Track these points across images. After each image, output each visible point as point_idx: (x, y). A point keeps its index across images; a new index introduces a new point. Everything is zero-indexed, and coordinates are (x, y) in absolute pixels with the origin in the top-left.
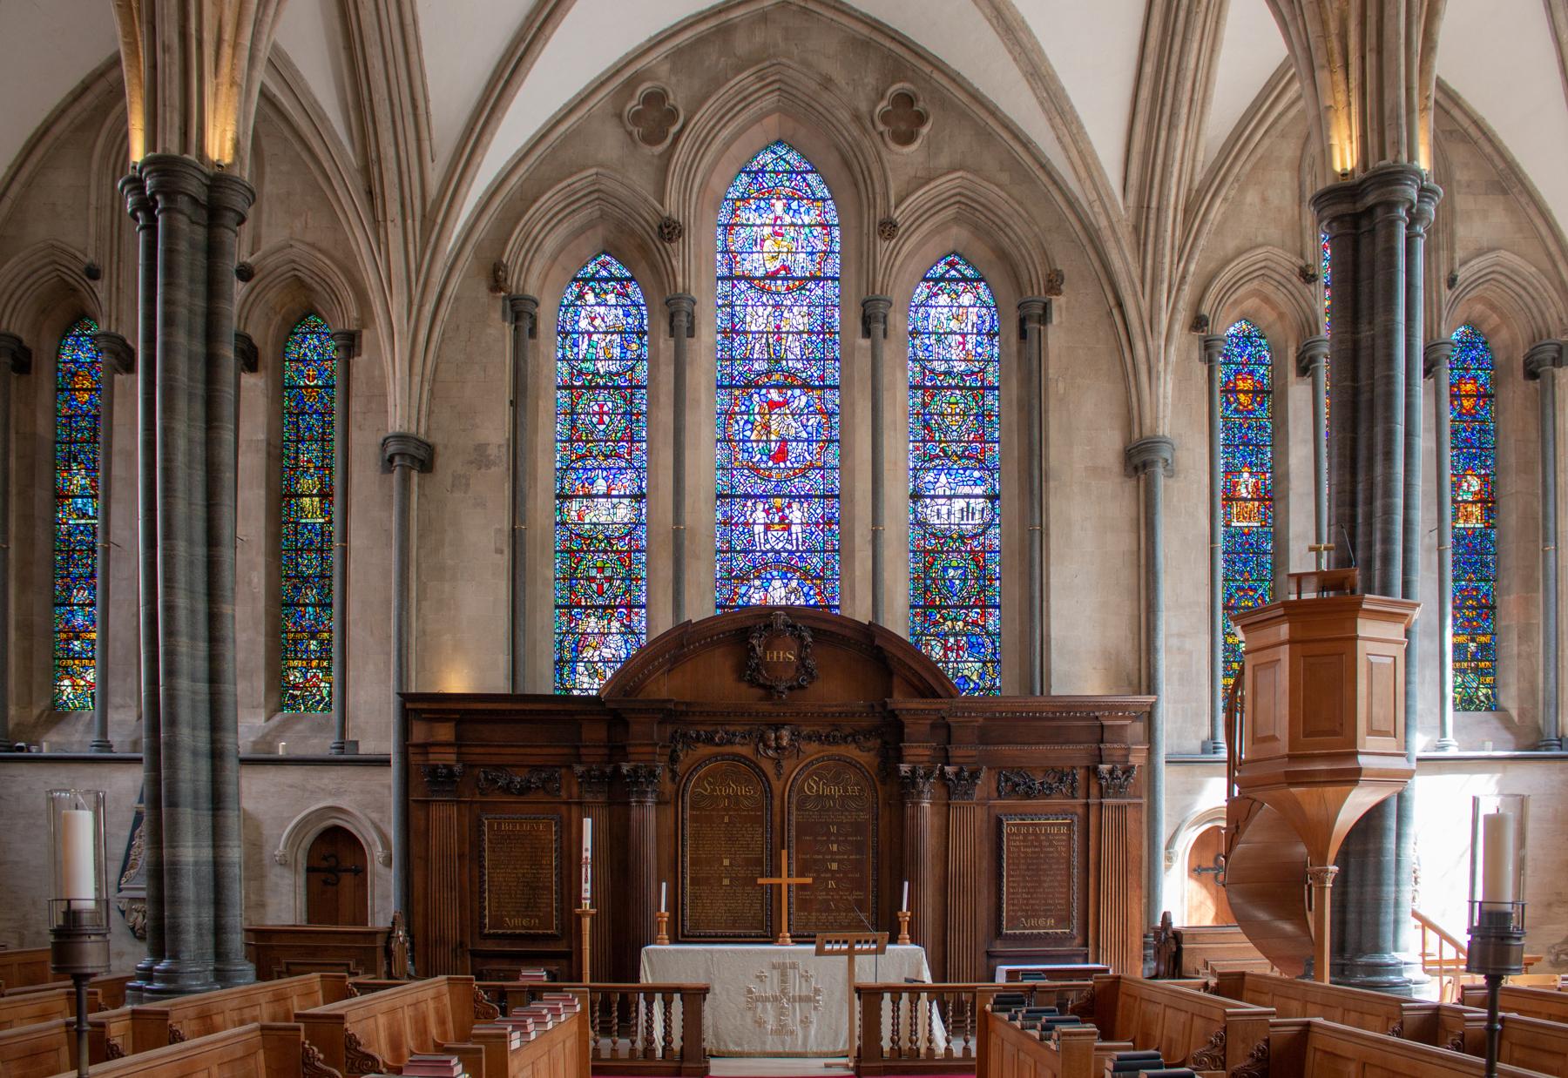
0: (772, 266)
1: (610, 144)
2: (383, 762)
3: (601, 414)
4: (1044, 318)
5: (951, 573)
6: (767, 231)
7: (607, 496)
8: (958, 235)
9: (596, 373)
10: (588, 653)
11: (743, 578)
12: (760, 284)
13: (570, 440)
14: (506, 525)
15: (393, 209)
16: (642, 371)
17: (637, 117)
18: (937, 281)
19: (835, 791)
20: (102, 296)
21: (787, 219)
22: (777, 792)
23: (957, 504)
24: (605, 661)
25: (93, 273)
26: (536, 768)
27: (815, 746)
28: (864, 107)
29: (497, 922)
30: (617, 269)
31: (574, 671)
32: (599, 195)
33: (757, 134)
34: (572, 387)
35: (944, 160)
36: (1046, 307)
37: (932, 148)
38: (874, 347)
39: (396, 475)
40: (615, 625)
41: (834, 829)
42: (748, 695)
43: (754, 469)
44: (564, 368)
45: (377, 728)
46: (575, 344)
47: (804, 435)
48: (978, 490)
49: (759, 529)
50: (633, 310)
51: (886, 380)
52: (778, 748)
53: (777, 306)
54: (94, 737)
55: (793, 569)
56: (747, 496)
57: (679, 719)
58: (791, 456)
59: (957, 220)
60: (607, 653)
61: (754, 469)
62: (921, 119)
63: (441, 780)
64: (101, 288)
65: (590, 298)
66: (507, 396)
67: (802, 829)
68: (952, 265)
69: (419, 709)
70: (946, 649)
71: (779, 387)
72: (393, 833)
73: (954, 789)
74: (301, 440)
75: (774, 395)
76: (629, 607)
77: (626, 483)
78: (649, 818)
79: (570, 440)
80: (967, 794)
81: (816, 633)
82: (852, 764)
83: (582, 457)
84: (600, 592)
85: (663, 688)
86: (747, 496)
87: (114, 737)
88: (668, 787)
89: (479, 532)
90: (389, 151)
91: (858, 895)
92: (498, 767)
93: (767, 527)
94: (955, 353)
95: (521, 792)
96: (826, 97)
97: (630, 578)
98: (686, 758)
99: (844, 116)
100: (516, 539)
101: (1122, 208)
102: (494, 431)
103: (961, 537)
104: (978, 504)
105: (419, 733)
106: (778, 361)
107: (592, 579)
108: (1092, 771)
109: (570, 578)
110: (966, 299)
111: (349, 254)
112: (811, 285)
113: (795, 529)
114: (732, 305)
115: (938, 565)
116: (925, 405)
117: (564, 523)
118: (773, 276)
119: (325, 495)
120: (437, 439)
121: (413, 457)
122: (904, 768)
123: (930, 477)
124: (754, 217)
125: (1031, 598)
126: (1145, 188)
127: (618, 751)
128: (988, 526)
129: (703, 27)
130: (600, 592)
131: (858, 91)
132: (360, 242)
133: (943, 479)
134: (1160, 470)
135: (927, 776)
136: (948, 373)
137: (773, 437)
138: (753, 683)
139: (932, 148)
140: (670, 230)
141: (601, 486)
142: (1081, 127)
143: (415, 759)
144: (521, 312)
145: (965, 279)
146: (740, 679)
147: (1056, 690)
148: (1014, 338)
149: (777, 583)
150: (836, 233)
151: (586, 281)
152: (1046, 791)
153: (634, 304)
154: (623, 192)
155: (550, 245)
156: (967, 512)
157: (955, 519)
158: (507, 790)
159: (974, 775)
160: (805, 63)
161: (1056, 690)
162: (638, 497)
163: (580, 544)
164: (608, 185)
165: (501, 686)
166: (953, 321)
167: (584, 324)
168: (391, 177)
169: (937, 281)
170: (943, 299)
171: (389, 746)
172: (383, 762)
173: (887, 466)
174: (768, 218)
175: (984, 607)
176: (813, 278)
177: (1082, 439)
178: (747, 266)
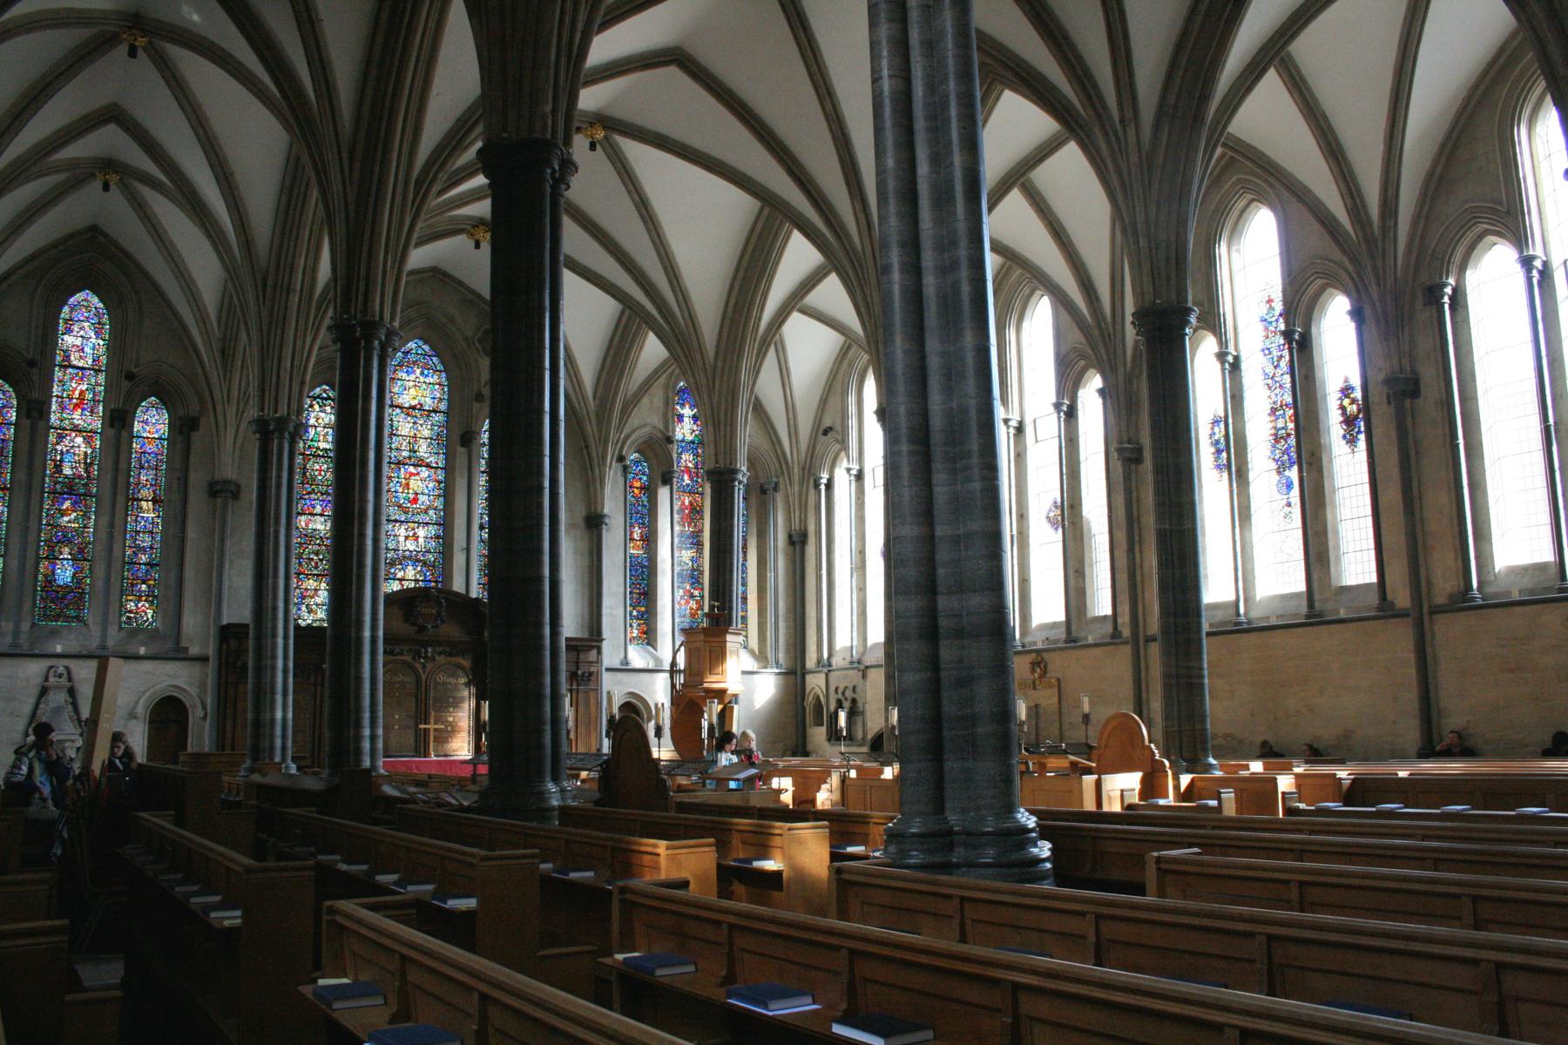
0: (414, 403)
10: (306, 601)
22: (423, 677)
42: (409, 630)
43: (400, 506)
49: (402, 539)
52: (426, 657)
61: (400, 506)
65: (317, 407)
71: (415, 466)
74: (142, 467)
75: (412, 469)
93: (407, 538)
113: (421, 540)
118: (413, 408)
124: (404, 376)
141: (318, 509)
172: (204, 659)
174: (412, 377)
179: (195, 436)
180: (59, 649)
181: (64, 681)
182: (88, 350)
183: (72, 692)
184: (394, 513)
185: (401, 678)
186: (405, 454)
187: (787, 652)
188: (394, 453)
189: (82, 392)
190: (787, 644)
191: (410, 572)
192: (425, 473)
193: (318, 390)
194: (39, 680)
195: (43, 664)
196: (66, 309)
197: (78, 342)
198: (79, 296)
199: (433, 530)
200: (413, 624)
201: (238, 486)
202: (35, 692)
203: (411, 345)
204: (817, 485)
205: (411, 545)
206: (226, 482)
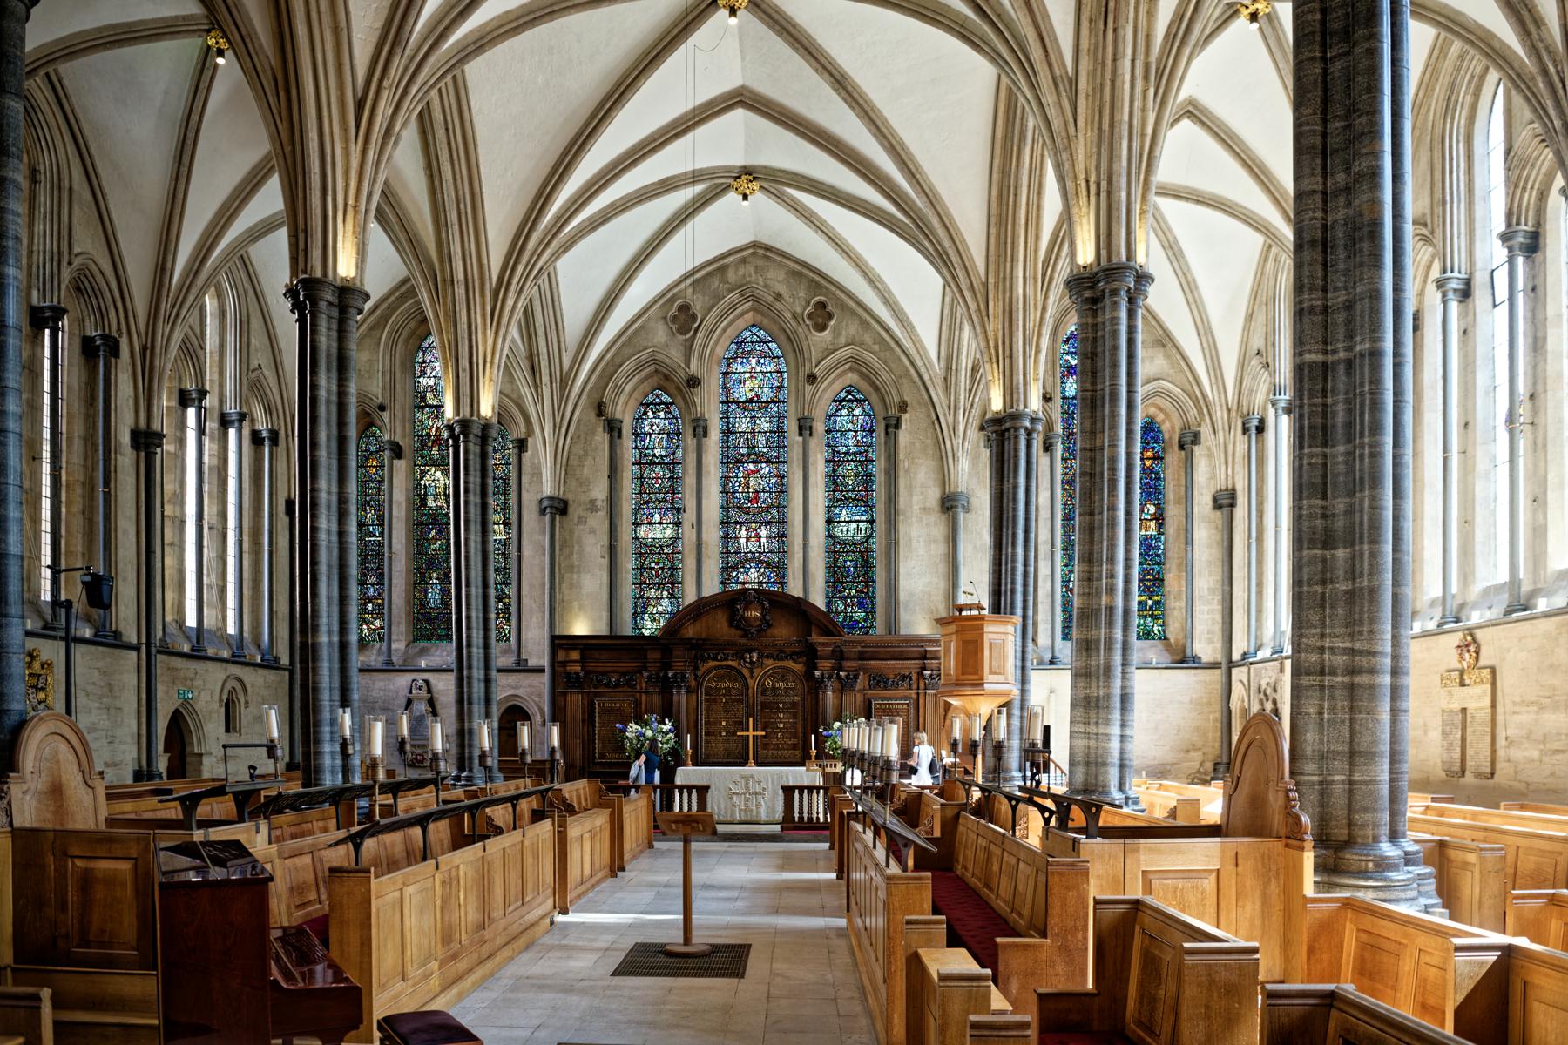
0: (750, 395)
1: (660, 334)
2: (541, 670)
4: (897, 426)
8: (852, 378)
10: (650, 609)
11: (735, 567)
12: (744, 405)
14: (606, 542)
15: (545, 379)
17: (674, 319)
19: (781, 685)
20: (387, 420)
23: (851, 527)
25: (382, 408)
26: (623, 674)
27: (771, 661)
28: (799, 310)
29: (602, 756)
30: (665, 398)
32: (653, 361)
33: (741, 323)
35: (843, 340)
36: (899, 420)
37: (836, 333)
39: (547, 517)
45: (537, 651)
49: (743, 541)
51: (811, 460)
52: (752, 662)
54: (382, 658)
55: (762, 562)
56: (737, 523)
57: (702, 648)
59: (851, 369)
63: (573, 682)
64: (386, 415)
65: (650, 414)
66: (606, 473)
67: (765, 705)
69: (560, 643)
72: (546, 709)
73: (845, 686)
75: (751, 466)
76: (673, 583)
77: (670, 517)
80: (852, 687)
81: (772, 602)
82: (792, 671)
85: (690, 632)
86: (737, 523)
87: (394, 659)
88: (693, 683)
89: (593, 545)
90: (543, 350)
91: (794, 741)
92: (604, 673)
93: (748, 539)
94: (851, 442)
95: (618, 685)
96: (778, 305)
97: (673, 568)
98: (703, 668)
99: (788, 315)
100: (612, 551)
101: (938, 368)
102: (600, 492)
104: (863, 525)
105: (561, 656)
108: (920, 675)
109: (640, 568)
110: (857, 412)
111: (520, 397)
113: (763, 540)
117: (637, 538)
118: (750, 401)
119: (506, 524)
120: (569, 497)
121: (558, 508)
122: (817, 673)
126: (949, 359)
127: (667, 666)
128: (868, 538)
129: (710, 269)
131: (796, 301)
132: (527, 393)
134: (960, 510)
135: (830, 677)
136: (847, 453)
139: (836, 333)
140: (694, 382)
141: (657, 518)
142: (913, 328)
143: (559, 669)
144: (613, 428)
146: (731, 625)
147: (903, 631)
152: (896, 685)
154: (667, 360)
155: (628, 388)
156: (858, 530)
158: (607, 686)
159: (856, 677)
160: (766, 286)
161: (903, 631)
162: (678, 524)
163: (644, 550)
164: (659, 357)
165: (603, 630)
167: (647, 429)
168: (544, 363)
170: (844, 412)
172: (542, 670)
173: (811, 506)
175: (866, 582)
177: (918, 491)
179: (526, 457)
180: (423, 665)
181: (423, 693)
183: (431, 702)
185: (727, 684)
191: (753, 575)
194: (406, 692)
195: (409, 677)
197: (431, 382)
201: (566, 503)
202: (404, 701)
205: (753, 546)
206: (551, 498)
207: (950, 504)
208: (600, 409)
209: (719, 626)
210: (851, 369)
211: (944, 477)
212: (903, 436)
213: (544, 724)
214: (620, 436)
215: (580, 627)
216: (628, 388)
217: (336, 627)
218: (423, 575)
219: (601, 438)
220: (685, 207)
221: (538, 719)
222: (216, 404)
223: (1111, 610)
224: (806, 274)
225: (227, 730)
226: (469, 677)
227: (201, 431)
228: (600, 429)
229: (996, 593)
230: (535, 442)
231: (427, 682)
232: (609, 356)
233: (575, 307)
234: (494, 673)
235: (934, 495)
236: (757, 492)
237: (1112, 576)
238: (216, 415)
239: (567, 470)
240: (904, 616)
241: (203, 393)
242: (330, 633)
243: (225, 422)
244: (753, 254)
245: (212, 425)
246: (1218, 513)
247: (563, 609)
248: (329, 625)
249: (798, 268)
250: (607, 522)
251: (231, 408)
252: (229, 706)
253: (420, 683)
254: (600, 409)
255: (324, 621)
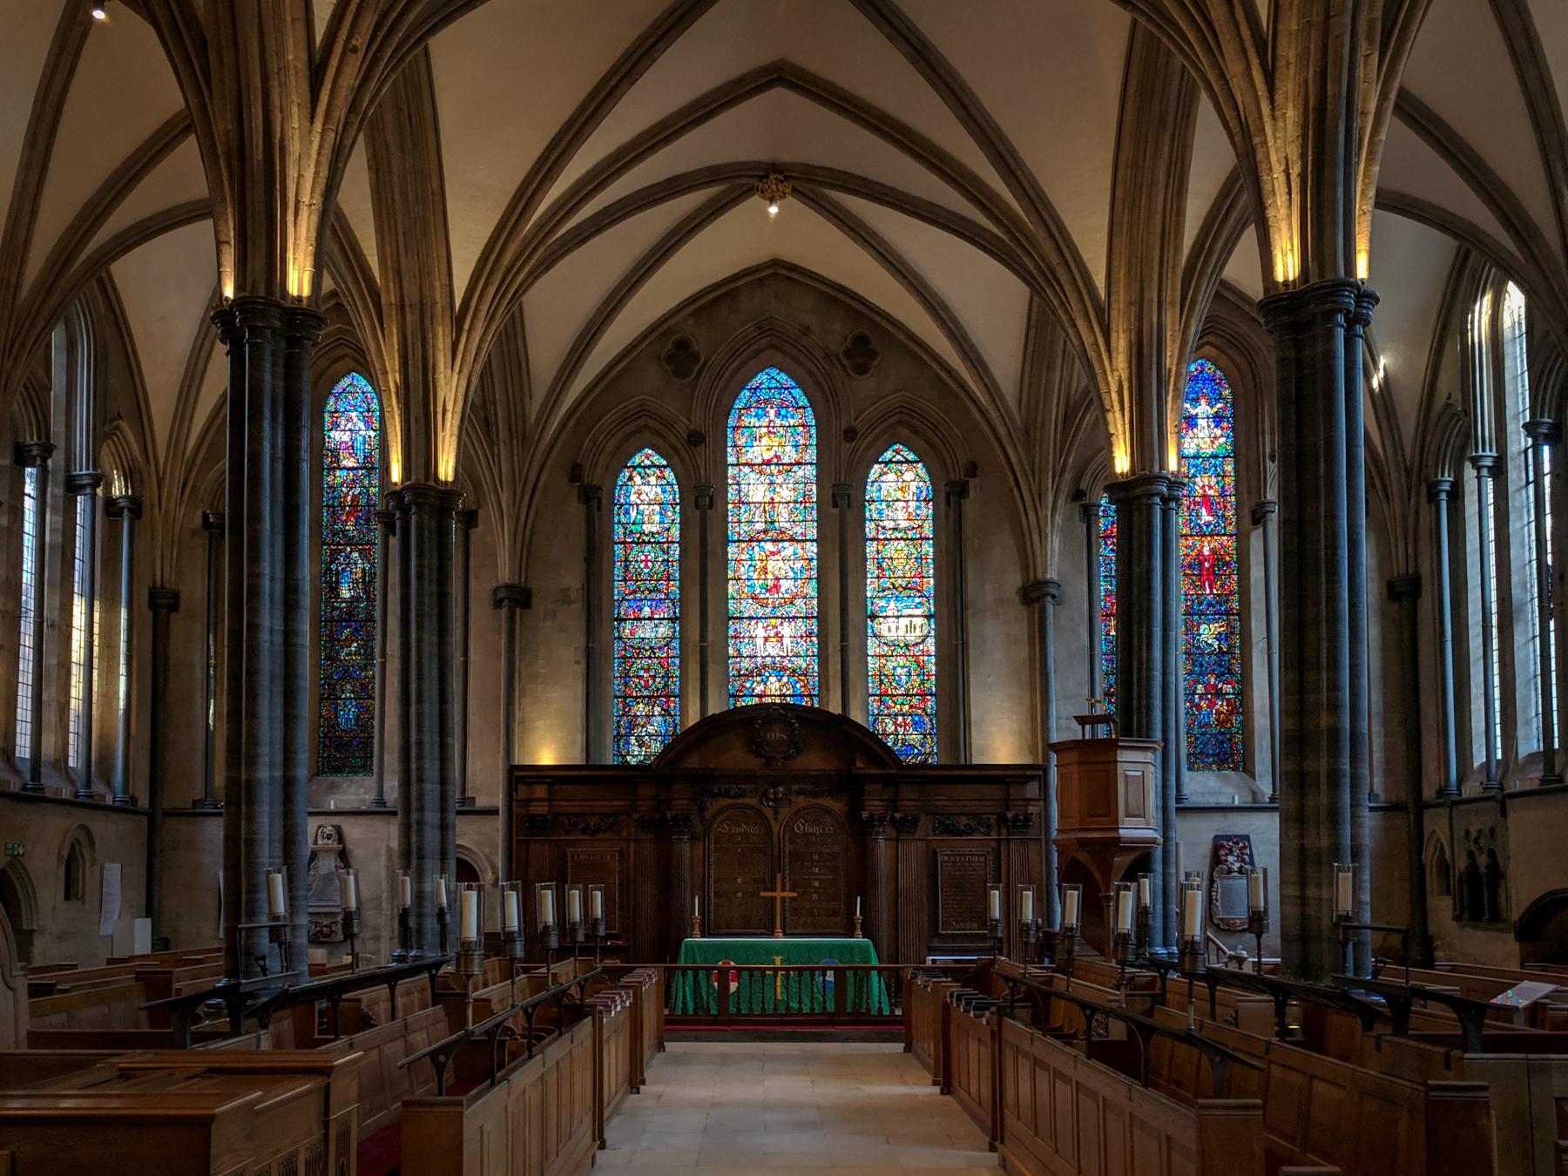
0: (768, 455)
3: (646, 561)
5: (899, 671)
6: (764, 430)
7: (651, 619)
9: (642, 533)
10: (637, 731)
11: (749, 675)
13: (625, 580)
14: (580, 641)
16: (675, 532)
18: (886, 463)
21: (778, 422)
24: (650, 735)
31: (628, 743)
34: (625, 543)
38: (841, 513)
40: (657, 710)
41: (816, 857)
42: (753, 763)
44: (621, 531)
46: (627, 512)
47: (791, 575)
48: (919, 612)
49: (760, 641)
50: (668, 488)
53: (771, 483)
55: (784, 669)
56: (751, 618)
57: (705, 783)
58: (783, 589)
60: (651, 729)
61: (755, 598)
62: (873, 355)
65: (638, 479)
68: (897, 452)
70: (895, 724)
71: (774, 541)
75: (769, 546)
78: (686, 850)
79: (625, 580)
83: (634, 592)
84: (647, 687)
93: (766, 639)
94: (901, 515)
103: (907, 646)
104: (918, 621)
106: (772, 522)
107: (640, 677)
109: (626, 675)
110: (909, 476)
112: (795, 468)
113: (786, 641)
114: (738, 484)
115: (890, 665)
116: (878, 552)
117: (620, 638)
118: (768, 463)
123: (883, 603)
124: (753, 420)
125: (957, 692)
130: (647, 687)
133: (892, 604)
136: (895, 529)
137: (770, 576)
138: (759, 754)
141: (647, 611)
145: (907, 461)
148: (943, 505)
149: (773, 679)
150: (813, 431)
151: (635, 468)
153: (668, 484)
157: (902, 632)
166: (899, 491)
167: (633, 498)
169: (886, 463)
170: (891, 477)
171: (499, 801)
175: (923, 695)
176: (798, 463)
178: (750, 455)
179: (475, 534)
182: (358, 445)
184: (749, 608)
186: (760, 526)
187: (1388, 773)
188: (744, 527)
189: (354, 497)
190: (1387, 760)
192: (789, 549)
193: (637, 459)
196: (332, 400)
198: (345, 382)
199: (802, 627)
200: (762, 756)
203: (762, 377)
204: (1433, 498)
205: (772, 649)
206: (507, 587)
207: (1035, 594)
208: (575, 473)
209: (734, 756)
210: (900, 422)
211: (1027, 559)
212: (970, 507)
213: (495, 884)
214: (599, 509)
215: (547, 756)
216: (610, 447)
217: (279, 758)
218: (332, 687)
219: (576, 510)
220: (691, 217)
221: (488, 877)
222: (62, 463)
223: (1334, 733)
224: (839, 299)
225: (67, 898)
226: (420, 823)
227: (41, 499)
228: (575, 499)
229: (1126, 707)
230: (488, 514)
231: (338, 829)
232: (585, 404)
233: (546, 347)
234: (451, 816)
235: (1014, 580)
236: (778, 579)
237: (1334, 687)
238: (61, 476)
239: (526, 551)
240: (976, 739)
241: (48, 450)
242: (272, 765)
243: (72, 487)
244: (775, 275)
245: (55, 491)
246: (1395, 606)
247: (524, 730)
248: (271, 754)
249: (832, 292)
250: (584, 617)
251: (82, 470)
252: (71, 865)
253: (329, 830)
254: (575, 473)
255: (264, 749)
